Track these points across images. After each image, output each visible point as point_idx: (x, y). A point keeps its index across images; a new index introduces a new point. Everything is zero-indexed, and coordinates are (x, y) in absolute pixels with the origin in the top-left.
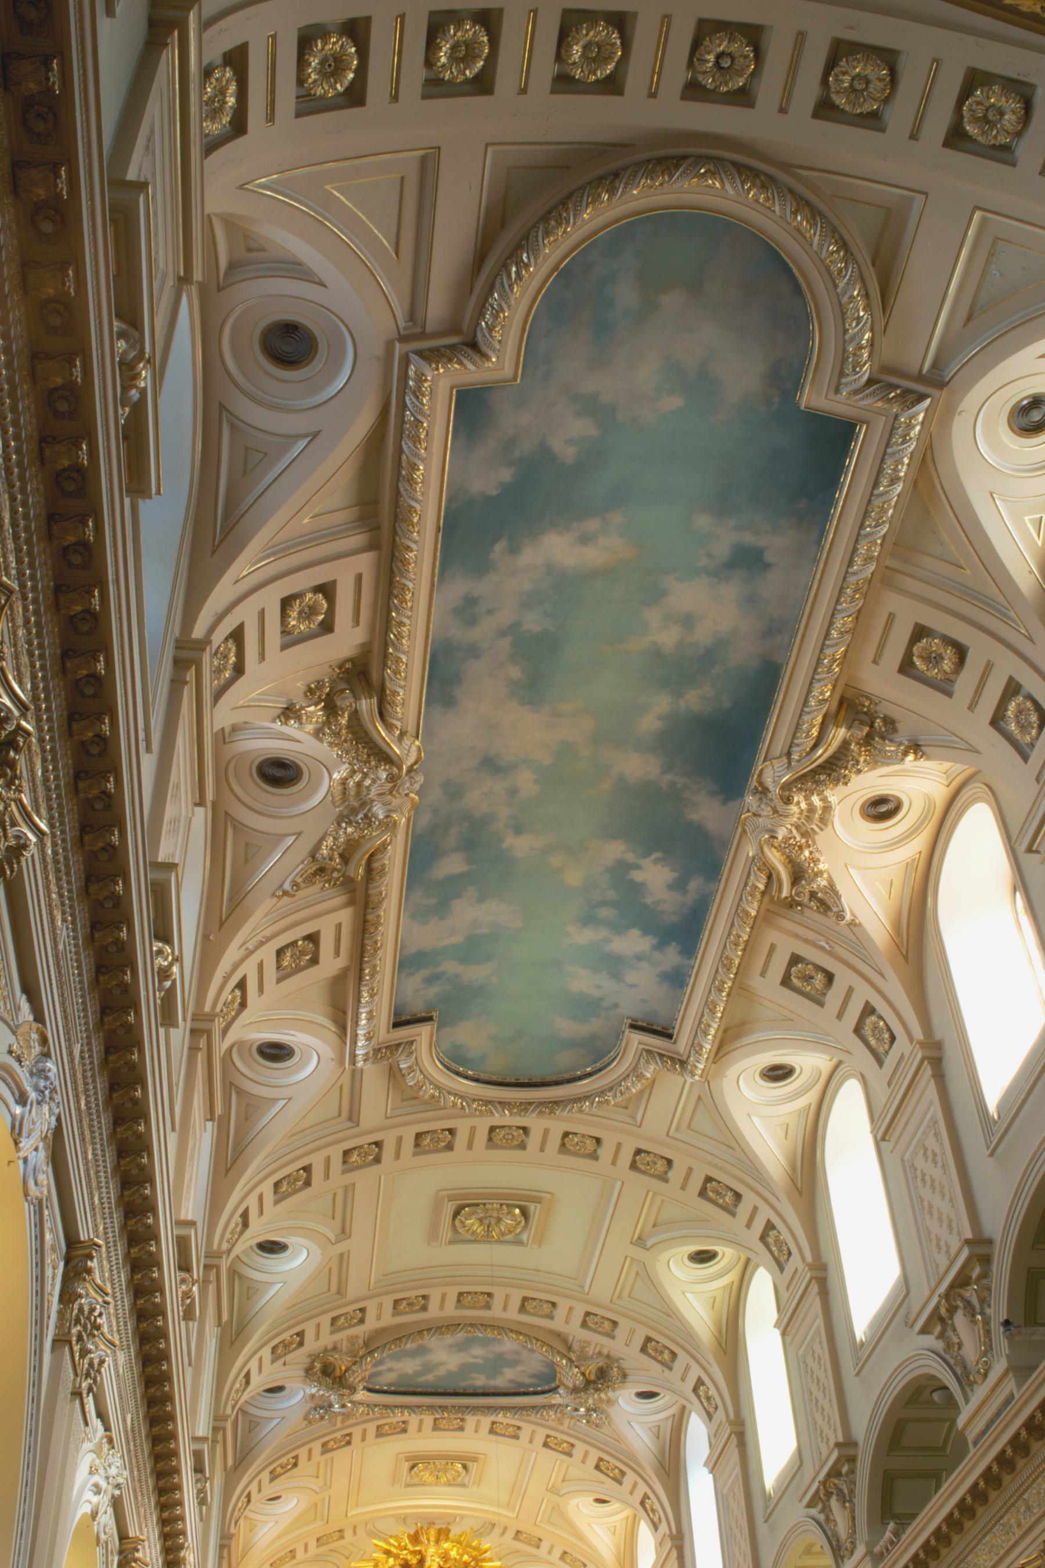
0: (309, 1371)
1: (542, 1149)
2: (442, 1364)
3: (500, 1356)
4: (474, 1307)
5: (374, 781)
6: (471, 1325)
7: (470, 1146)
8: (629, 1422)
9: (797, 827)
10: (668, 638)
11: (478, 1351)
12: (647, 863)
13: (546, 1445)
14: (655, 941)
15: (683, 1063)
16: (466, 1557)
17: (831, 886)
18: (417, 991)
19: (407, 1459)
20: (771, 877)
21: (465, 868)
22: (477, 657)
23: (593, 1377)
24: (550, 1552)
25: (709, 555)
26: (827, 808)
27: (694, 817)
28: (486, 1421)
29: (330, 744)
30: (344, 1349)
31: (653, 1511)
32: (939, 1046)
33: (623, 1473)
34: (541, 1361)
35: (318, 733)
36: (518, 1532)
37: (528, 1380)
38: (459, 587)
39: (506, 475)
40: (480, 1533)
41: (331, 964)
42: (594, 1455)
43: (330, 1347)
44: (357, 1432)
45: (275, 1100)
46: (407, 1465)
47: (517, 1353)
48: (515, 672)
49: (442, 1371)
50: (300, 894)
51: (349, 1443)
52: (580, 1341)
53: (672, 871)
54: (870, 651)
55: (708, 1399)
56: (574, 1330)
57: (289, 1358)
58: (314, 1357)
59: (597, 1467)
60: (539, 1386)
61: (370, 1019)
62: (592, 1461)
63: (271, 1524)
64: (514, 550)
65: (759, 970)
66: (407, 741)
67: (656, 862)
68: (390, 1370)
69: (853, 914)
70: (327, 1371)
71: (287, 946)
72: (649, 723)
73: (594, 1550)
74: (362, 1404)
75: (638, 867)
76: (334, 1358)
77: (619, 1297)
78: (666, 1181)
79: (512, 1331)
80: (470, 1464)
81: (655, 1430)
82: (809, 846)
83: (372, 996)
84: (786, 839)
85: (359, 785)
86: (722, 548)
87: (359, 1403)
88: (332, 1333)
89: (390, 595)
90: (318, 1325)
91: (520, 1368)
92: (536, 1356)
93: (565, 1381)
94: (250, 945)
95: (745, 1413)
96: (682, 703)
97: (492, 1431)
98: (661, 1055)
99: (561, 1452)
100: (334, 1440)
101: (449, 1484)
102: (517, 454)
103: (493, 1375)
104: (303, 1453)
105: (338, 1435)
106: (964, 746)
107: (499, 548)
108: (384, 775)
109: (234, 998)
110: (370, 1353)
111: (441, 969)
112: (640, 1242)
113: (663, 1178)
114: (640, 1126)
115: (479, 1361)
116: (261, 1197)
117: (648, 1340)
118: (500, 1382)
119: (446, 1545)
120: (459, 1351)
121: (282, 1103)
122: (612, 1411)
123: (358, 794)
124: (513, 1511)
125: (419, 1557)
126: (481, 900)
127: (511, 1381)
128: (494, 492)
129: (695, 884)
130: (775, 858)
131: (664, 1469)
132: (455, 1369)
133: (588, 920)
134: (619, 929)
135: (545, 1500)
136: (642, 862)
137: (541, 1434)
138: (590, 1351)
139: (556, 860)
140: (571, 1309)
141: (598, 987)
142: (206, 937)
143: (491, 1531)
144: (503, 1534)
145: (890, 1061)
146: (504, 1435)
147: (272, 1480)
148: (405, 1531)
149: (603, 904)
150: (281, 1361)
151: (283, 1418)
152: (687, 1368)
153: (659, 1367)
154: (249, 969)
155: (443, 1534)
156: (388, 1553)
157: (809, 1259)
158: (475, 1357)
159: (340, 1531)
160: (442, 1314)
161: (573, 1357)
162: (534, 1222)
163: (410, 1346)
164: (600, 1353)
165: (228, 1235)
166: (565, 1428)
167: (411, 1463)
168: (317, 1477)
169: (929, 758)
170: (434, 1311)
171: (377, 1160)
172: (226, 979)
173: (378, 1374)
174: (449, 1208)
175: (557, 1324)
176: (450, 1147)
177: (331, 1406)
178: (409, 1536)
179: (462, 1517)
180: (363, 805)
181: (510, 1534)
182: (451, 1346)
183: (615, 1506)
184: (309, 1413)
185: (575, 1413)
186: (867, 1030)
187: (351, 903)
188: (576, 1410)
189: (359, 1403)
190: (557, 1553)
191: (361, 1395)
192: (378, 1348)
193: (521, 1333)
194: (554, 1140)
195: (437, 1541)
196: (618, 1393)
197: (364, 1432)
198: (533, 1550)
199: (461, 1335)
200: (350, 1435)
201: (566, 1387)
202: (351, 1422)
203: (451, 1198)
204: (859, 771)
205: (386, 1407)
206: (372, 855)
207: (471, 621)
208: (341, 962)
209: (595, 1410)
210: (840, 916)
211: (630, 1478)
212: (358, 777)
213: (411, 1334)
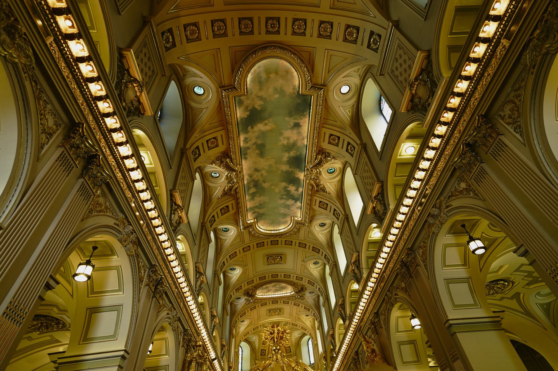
1: (281, 244)
5: (233, 175)
7: (267, 245)
9: (316, 176)
10: (285, 142)
12: (290, 186)
13: (294, 305)
14: (294, 201)
15: (304, 224)
16: (283, 330)
17: (324, 187)
19: (268, 310)
20: (312, 186)
21: (256, 191)
25: (290, 125)
26: (320, 172)
29: (223, 168)
32: (347, 215)
33: (309, 309)
35: (220, 166)
39: (248, 113)
40: (285, 325)
41: (232, 212)
42: (303, 306)
44: (257, 305)
45: (227, 239)
48: (257, 152)
50: (223, 198)
51: (256, 308)
54: (322, 140)
55: (321, 292)
56: (294, 280)
57: (239, 291)
58: (245, 291)
59: (304, 308)
61: (242, 221)
62: (303, 307)
64: (252, 128)
65: (314, 205)
66: (238, 166)
67: (292, 186)
71: (222, 208)
72: (285, 159)
73: (308, 326)
75: (288, 187)
78: (306, 248)
82: (318, 179)
83: (241, 217)
84: (314, 178)
85: (230, 176)
86: (292, 124)
88: (248, 285)
89: (229, 138)
90: (244, 284)
94: (214, 209)
95: (328, 294)
97: (283, 303)
98: (300, 223)
100: (253, 308)
101: (277, 315)
102: (249, 109)
104: (246, 311)
105: (253, 306)
108: (234, 173)
109: (212, 219)
111: (255, 211)
112: (303, 261)
113: (305, 248)
116: (227, 259)
119: (279, 328)
121: (228, 240)
122: (305, 296)
123: (230, 178)
128: (246, 117)
130: (312, 182)
133: (282, 198)
134: (288, 200)
136: (289, 186)
137: (293, 302)
138: (299, 284)
139: (273, 187)
140: (293, 276)
141: (286, 211)
142: (204, 208)
145: (340, 219)
147: (241, 317)
148: (270, 326)
150: (237, 293)
152: (317, 286)
154: (214, 213)
155: (278, 326)
157: (333, 261)
160: (269, 279)
162: (283, 259)
163: (264, 287)
165: (220, 267)
166: (297, 301)
169: (336, 159)
170: (267, 279)
171: (250, 250)
172: (210, 216)
174: (266, 258)
175: (291, 279)
176: (264, 246)
177: (250, 300)
179: (282, 322)
180: (232, 180)
181: (291, 324)
182: (272, 286)
183: (310, 316)
184: (246, 303)
186: (335, 214)
187: (234, 199)
190: (301, 327)
194: (283, 243)
195: (277, 327)
196: (305, 292)
197: (258, 305)
198: (296, 327)
199: (273, 284)
203: (266, 256)
204: (324, 164)
208: (234, 211)
210: (327, 192)
211: (311, 310)
212: (230, 174)
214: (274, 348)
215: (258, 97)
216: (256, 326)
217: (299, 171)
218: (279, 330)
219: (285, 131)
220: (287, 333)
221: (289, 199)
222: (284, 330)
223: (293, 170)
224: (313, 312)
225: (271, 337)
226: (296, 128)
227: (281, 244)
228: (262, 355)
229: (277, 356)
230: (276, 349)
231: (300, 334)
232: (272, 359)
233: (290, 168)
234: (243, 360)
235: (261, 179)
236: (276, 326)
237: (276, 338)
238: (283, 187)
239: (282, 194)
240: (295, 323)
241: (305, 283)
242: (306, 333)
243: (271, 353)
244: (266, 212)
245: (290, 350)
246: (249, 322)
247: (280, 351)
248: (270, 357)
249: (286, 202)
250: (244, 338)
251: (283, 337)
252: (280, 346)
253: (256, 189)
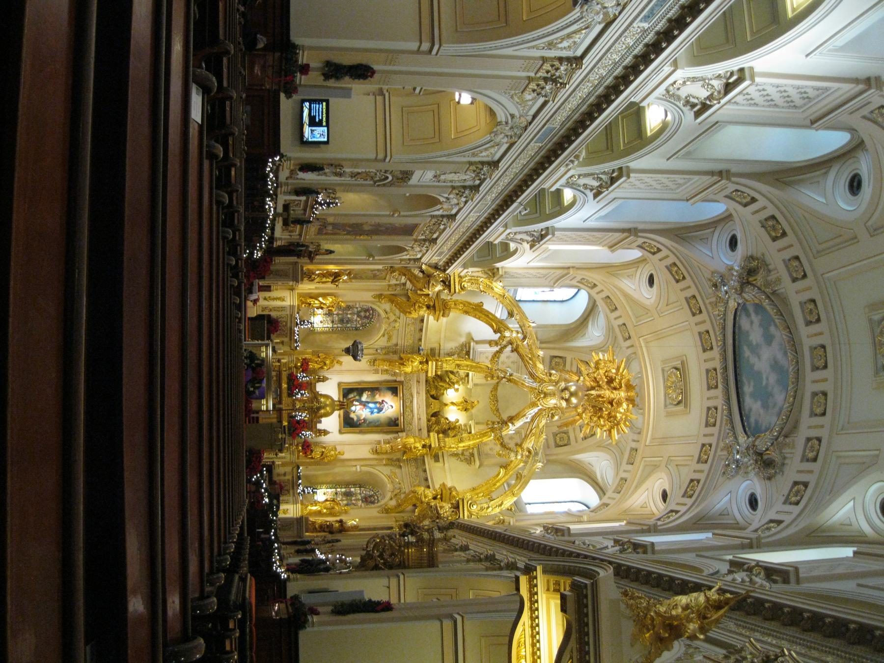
0: (752, 258)
2: (759, 357)
3: (771, 395)
4: (812, 358)
6: (797, 362)
8: (730, 492)
11: (773, 378)
23: (765, 457)
24: (625, 471)
28: (720, 402)
30: (769, 278)
31: (669, 517)
34: (770, 424)
36: (636, 450)
37: (752, 420)
40: (632, 427)
42: (702, 477)
43: (771, 267)
44: (704, 316)
46: (678, 363)
47: (775, 405)
49: (753, 360)
51: (694, 314)
52: (793, 441)
59: (692, 481)
60: (749, 428)
63: (633, 287)
68: (752, 323)
70: (751, 272)
73: (630, 496)
74: (725, 311)
76: (762, 273)
77: (838, 457)
79: (796, 392)
80: (682, 405)
81: (725, 513)
87: (726, 307)
91: (762, 411)
92: (775, 419)
93: (758, 440)
99: (700, 455)
103: (753, 395)
104: (688, 282)
110: (768, 297)
115: (764, 383)
117: (806, 485)
118: (748, 401)
120: (771, 366)
122: (739, 478)
124: (650, 442)
125: (618, 387)
127: (750, 410)
131: (698, 521)
132: (756, 368)
135: (661, 459)
137: (713, 440)
138: (786, 450)
143: (634, 433)
144: (634, 441)
146: (707, 416)
151: (713, 258)
153: (786, 492)
156: (618, 369)
158: (767, 379)
159: (630, 337)
161: (781, 439)
164: (785, 458)
166: (719, 453)
167: (680, 366)
168: (667, 305)
173: (748, 315)
175: (806, 420)
178: (629, 380)
179: (643, 414)
181: (634, 445)
185: (735, 452)
188: (738, 452)
189: (726, 307)
190: (624, 475)
191: (732, 305)
192: (773, 301)
193: (795, 399)
200: (701, 312)
201: (755, 441)
202: (710, 308)
205: (724, 328)
209: (737, 466)
211: (689, 502)
213: (785, 321)
214: (573, 389)
216: (632, 333)
218: (619, 404)
220: (610, 431)
222: (618, 424)
224: (683, 509)
225: (601, 378)
228: (551, 362)
229: (553, 394)
230: (572, 394)
231: (602, 478)
232: (546, 379)
234: (540, 304)
236: (632, 394)
237: (599, 396)
240: (638, 458)
241: (794, 470)
242: (609, 493)
243: (560, 376)
245: (561, 443)
246: (648, 303)
247: (564, 404)
248: (551, 375)
250: (598, 298)
251: (599, 418)
252: (576, 407)
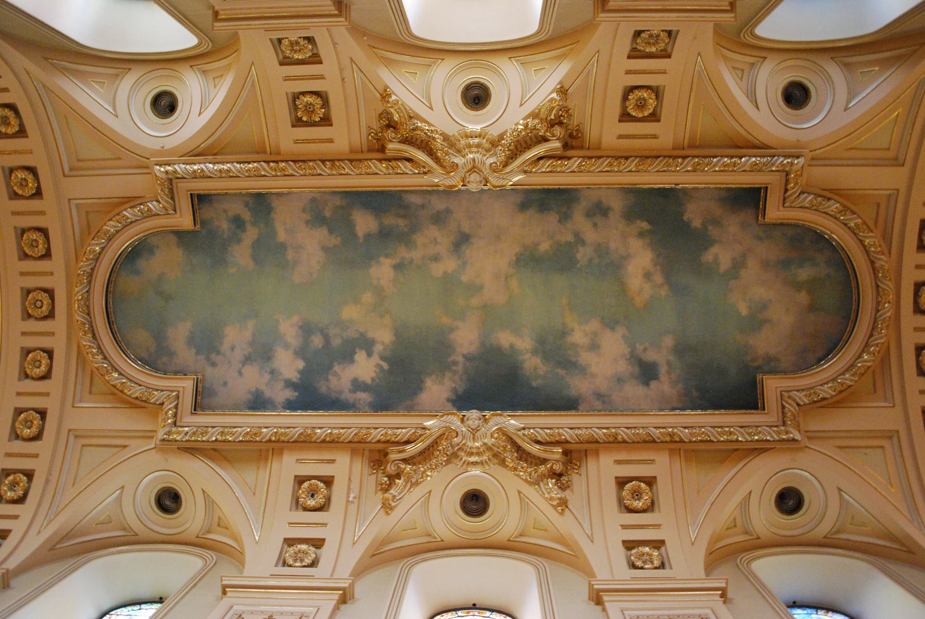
1: (23, 334)
7: (23, 274)
10: (578, 337)
12: (375, 359)
14: (294, 380)
18: (225, 211)
22: (560, 221)
25: (645, 350)
27: (429, 383)
38: (617, 204)
39: (697, 223)
53: (373, 379)
64: (641, 235)
67: (378, 365)
69: (397, 505)
72: (505, 339)
75: (369, 355)
86: (651, 356)
96: (527, 356)
102: (710, 228)
106: (589, 533)
107: (645, 225)
111: (249, 227)
114: (73, 407)
126: (326, 249)
129: (364, 396)
133: (307, 329)
134: (301, 353)
139: (368, 298)
141: (233, 348)
149: (327, 338)
187: (352, 151)
206: (409, 160)
207: (589, 214)
215: (744, 256)
217: (454, 390)
219: (623, 336)
221: (304, 359)
223: (460, 368)
226: (637, 370)
227: (23, 334)
233: (464, 356)
235: (416, 255)
238: (370, 335)
239: (333, 332)
244: (232, 270)
249: (286, 346)
253: (368, 237)
